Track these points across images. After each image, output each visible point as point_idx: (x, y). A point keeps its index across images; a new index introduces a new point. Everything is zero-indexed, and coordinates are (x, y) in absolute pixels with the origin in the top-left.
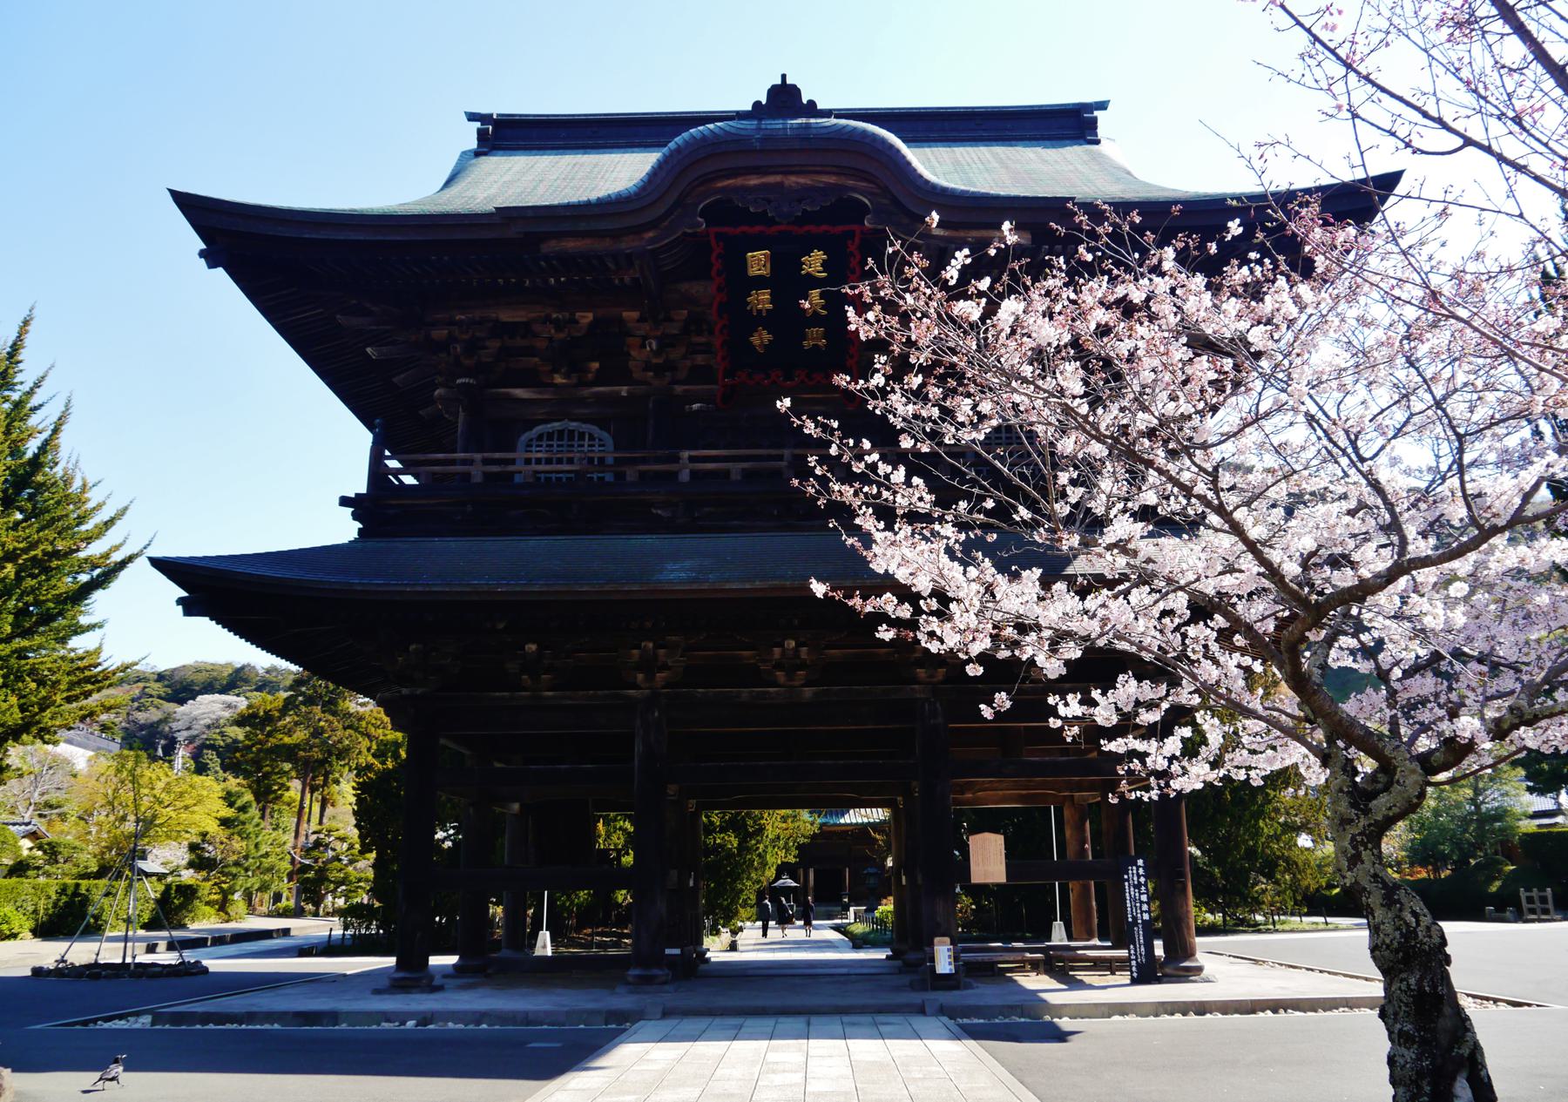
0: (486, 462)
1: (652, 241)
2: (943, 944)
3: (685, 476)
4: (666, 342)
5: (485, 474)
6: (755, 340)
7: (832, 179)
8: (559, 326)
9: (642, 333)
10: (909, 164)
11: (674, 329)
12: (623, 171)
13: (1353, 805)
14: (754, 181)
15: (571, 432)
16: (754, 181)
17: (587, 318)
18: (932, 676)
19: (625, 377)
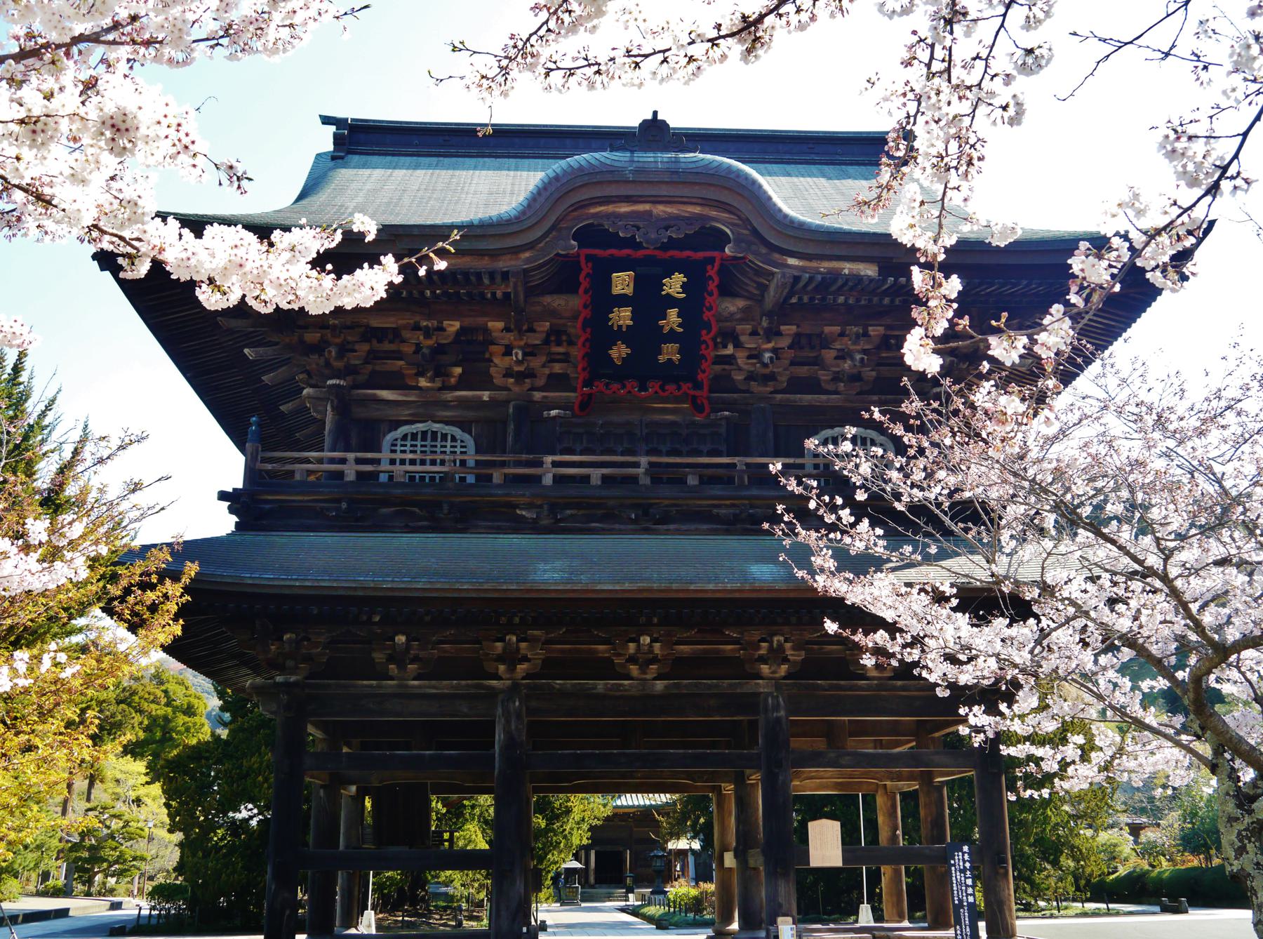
0: (359, 461)
1: (528, 261)
2: (786, 923)
3: (548, 480)
4: (530, 352)
5: (360, 475)
6: (614, 353)
7: (697, 210)
8: (428, 333)
9: (506, 342)
10: (770, 198)
11: (536, 340)
12: (493, 193)
13: (1240, 806)
14: (624, 209)
15: (434, 434)
16: (624, 209)
17: (453, 326)
18: (773, 672)
19: (487, 383)
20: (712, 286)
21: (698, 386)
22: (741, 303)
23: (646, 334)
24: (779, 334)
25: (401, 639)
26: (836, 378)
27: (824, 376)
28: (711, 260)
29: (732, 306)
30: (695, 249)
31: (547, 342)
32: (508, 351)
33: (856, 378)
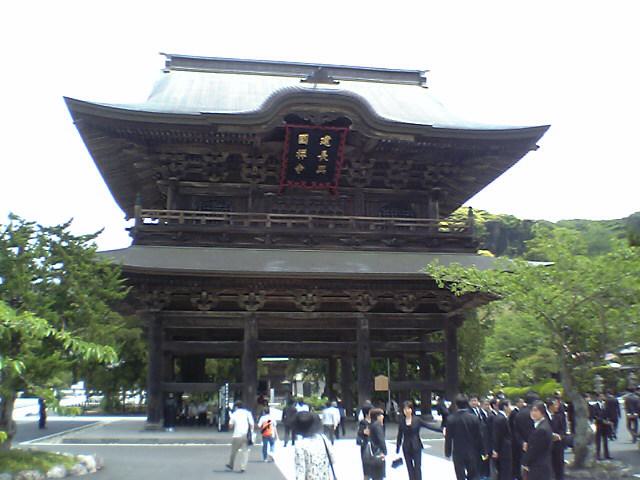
6: (297, 169)
11: (262, 161)
14: (306, 108)
16: (306, 108)
17: (226, 155)
20: (343, 142)
21: (333, 185)
22: (353, 148)
23: (311, 162)
24: (368, 162)
25: (204, 294)
26: (392, 182)
27: (386, 181)
28: (343, 131)
29: (349, 149)
30: (335, 126)
31: (267, 163)
32: (250, 166)
33: (401, 182)
